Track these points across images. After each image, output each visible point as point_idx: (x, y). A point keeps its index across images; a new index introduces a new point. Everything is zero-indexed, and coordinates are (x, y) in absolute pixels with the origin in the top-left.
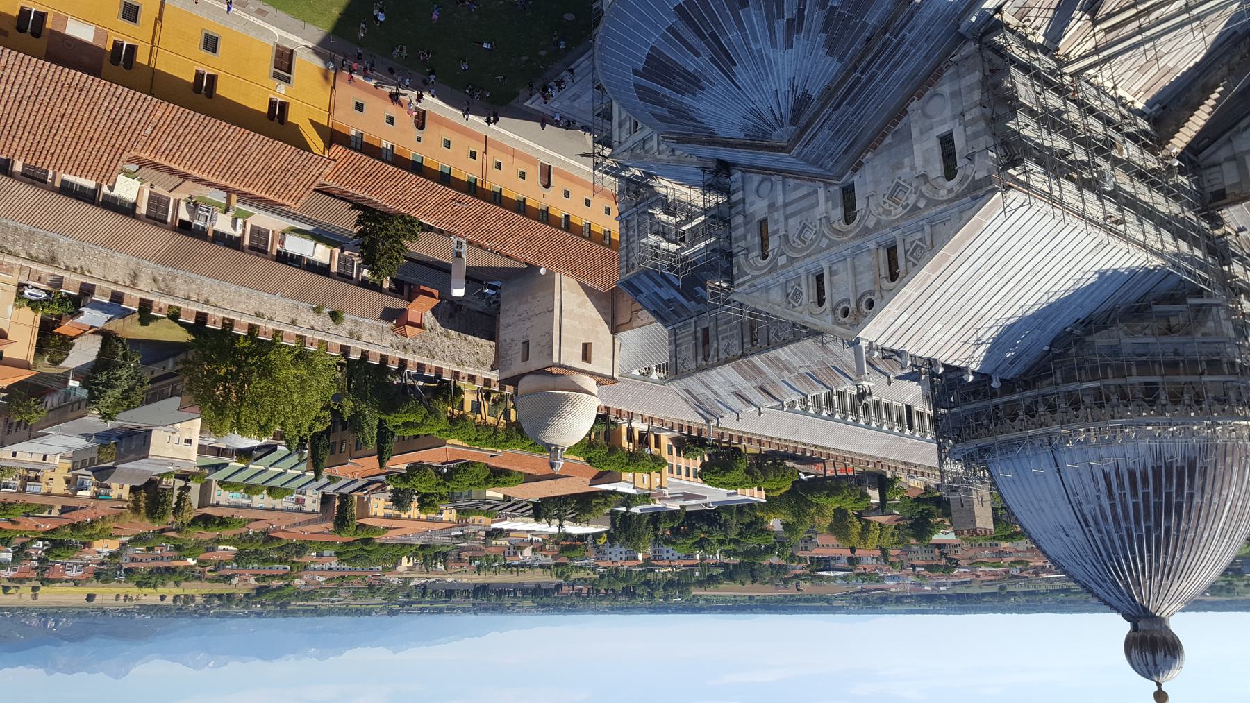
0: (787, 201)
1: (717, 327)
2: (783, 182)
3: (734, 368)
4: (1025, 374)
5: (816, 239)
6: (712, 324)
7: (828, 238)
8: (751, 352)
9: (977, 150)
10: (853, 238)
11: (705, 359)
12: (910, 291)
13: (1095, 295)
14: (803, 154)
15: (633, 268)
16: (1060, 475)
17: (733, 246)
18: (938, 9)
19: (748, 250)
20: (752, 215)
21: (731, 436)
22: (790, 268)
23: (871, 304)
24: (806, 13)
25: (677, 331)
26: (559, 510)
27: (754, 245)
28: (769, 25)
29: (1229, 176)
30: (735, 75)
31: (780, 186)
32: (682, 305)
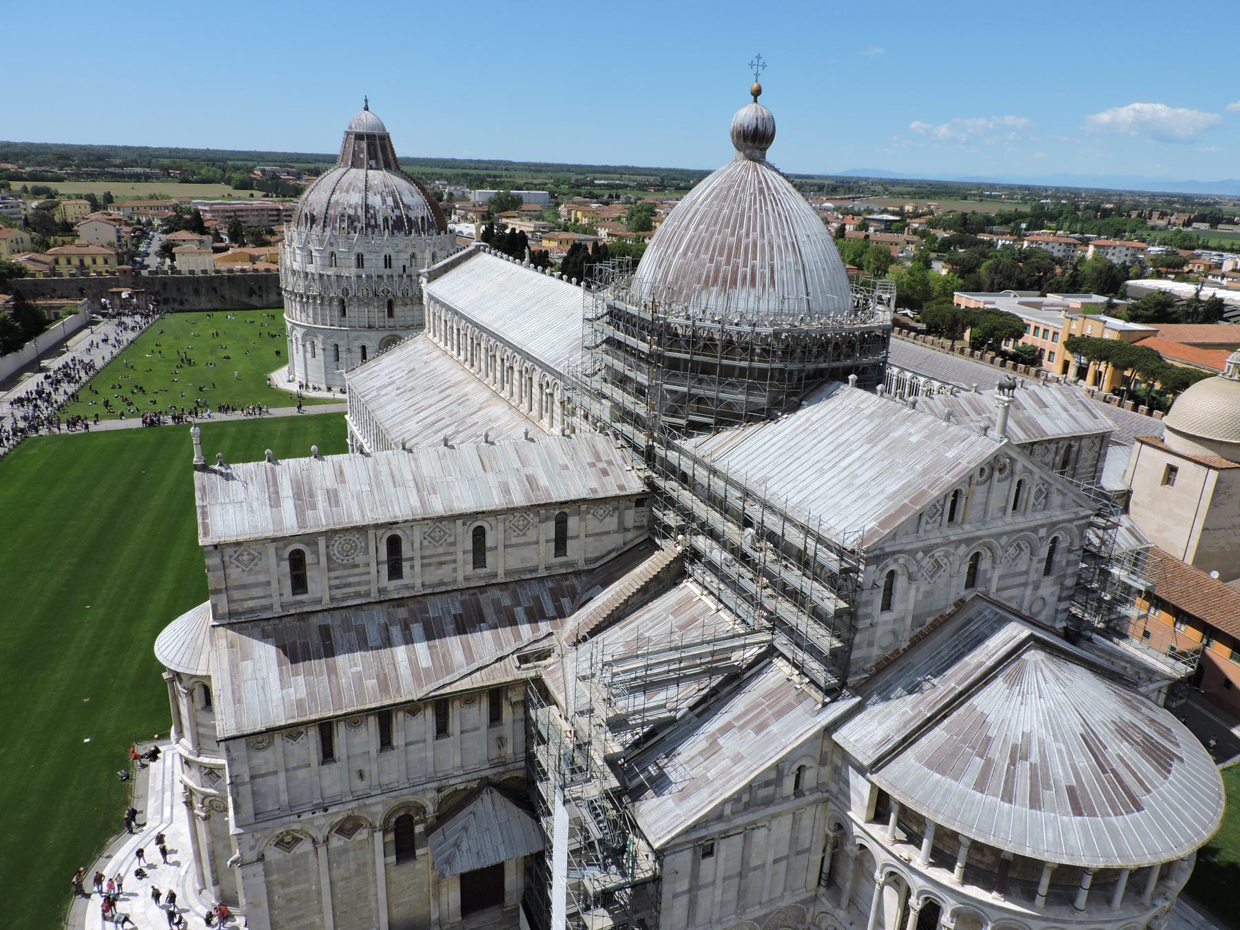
0: (1022, 588)
2: (1021, 606)
3: (1045, 433)
4: (823, 382)
9: (868, 592)
10: (980, 538)
11: (1070, 446)
12: (949, 479)
18: (880, 724)
19: (1069, 551)
20: (1055, 583)
22: (1040, 522)
23: (982, 470)
24: (1008, 761)
26: (1196, 308)
28: (1046, 762)
29: (631, 516)
30: (1082, 725)
31: (1026, 604)
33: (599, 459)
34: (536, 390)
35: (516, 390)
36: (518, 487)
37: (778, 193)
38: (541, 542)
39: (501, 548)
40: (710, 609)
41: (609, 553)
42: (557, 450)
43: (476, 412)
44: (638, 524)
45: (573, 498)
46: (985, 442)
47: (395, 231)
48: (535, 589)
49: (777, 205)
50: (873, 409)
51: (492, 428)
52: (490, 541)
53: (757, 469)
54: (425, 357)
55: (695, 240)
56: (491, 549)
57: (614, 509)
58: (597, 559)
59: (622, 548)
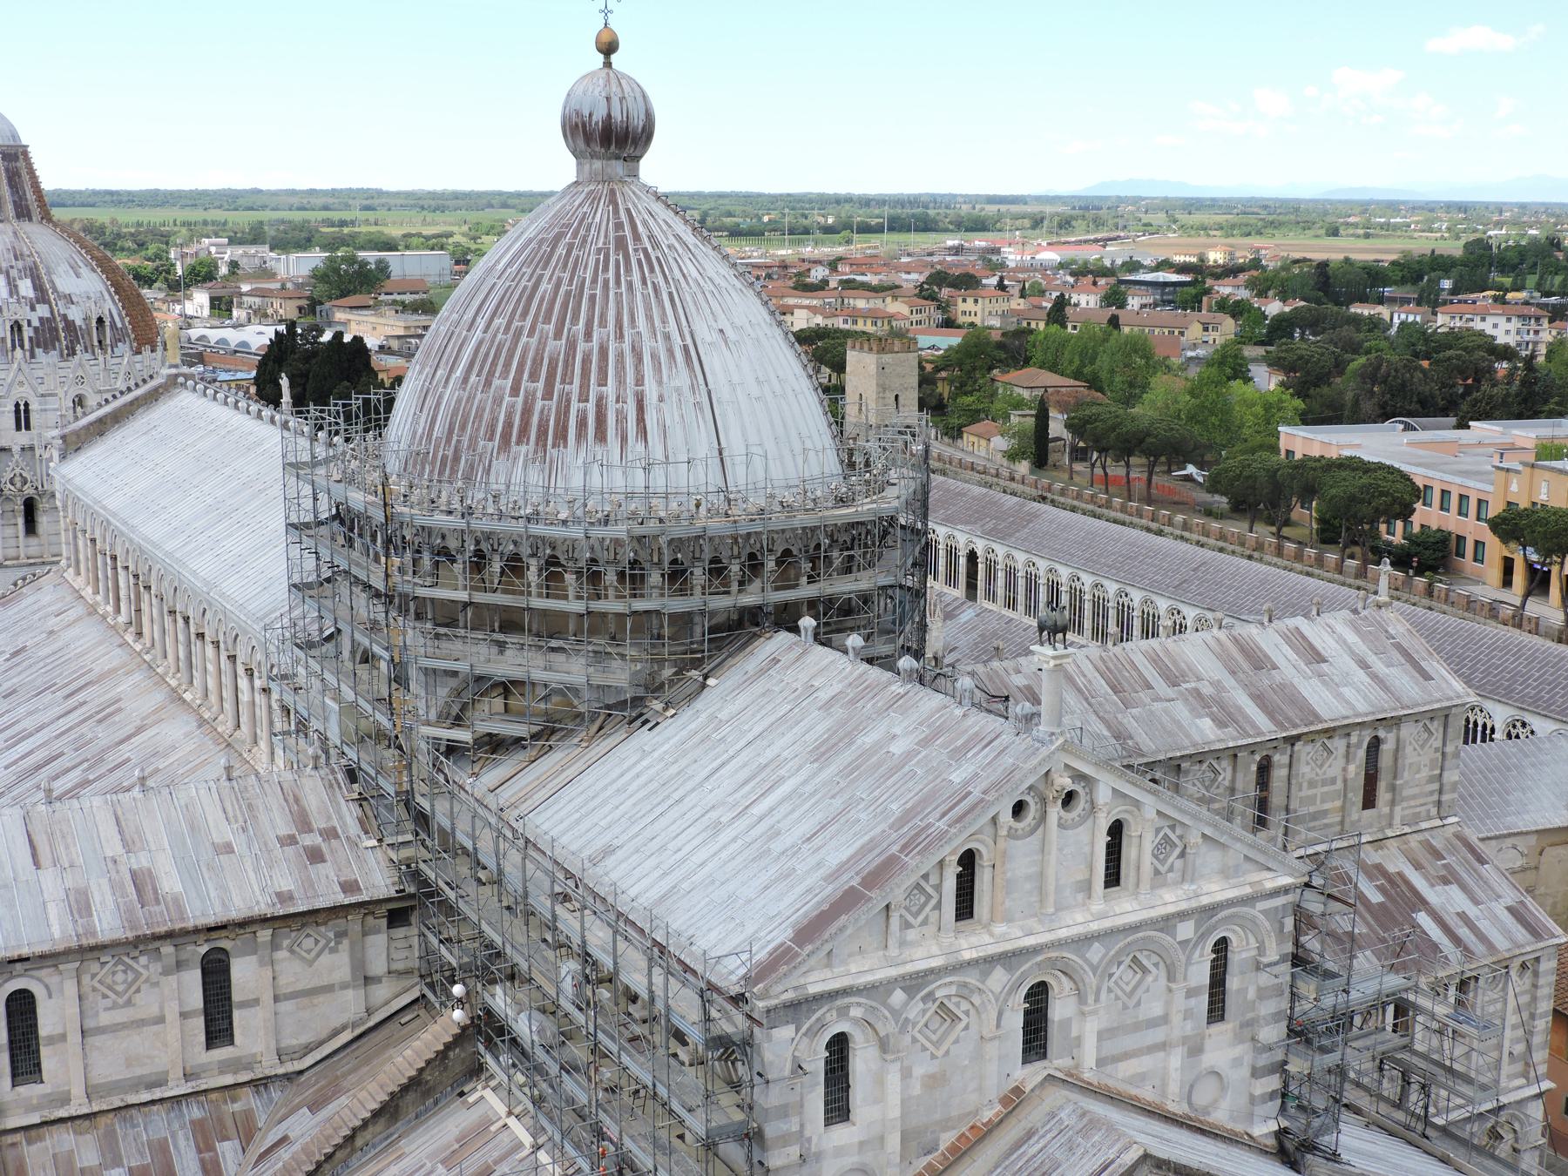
0: (1161, 1054)
1: (1343, 808)
2: (1164, 1094)
4: (756, 636)
5: (1111, 962)
6: (1355, 817)
7: (1086, 961)
8: (1275, 744)
11: (1375, 744)
13: (618, 771)
14: (1116, 1148)
15: (1524, 966)
16: (719, 444)
17: (1288, 978)
20: (1238, 1039)
21: (1340, 569)
22: (1171, 909)
23: (1019, 809)
25: (1434, 811)
27: (1243, 973)
32: (1418, 866)
33: (304, 824)
34: (243, 683)
35: (211, 684)
36: (109, 898)
37: (656, 245)
38: (169, 1018)
39: (74, 1038)
40: (520, 1145)
41: (335, 1033)
42: (213, 814)
43: (129, 737)
44: (400, 966)
45: (234, 915)
46: (1023, 746)
47: (38, 351)
48: (159, 1124)
49: (652, 270)
50: (837, 688)
51: (157, 771)
52: (47, 1023)
53: (597, 829)
54: (52, 622)
55: (483, 350)
56: (52, 1040)
57: (341, 935)
58: (308, 1049)
59: (362, 1021)
